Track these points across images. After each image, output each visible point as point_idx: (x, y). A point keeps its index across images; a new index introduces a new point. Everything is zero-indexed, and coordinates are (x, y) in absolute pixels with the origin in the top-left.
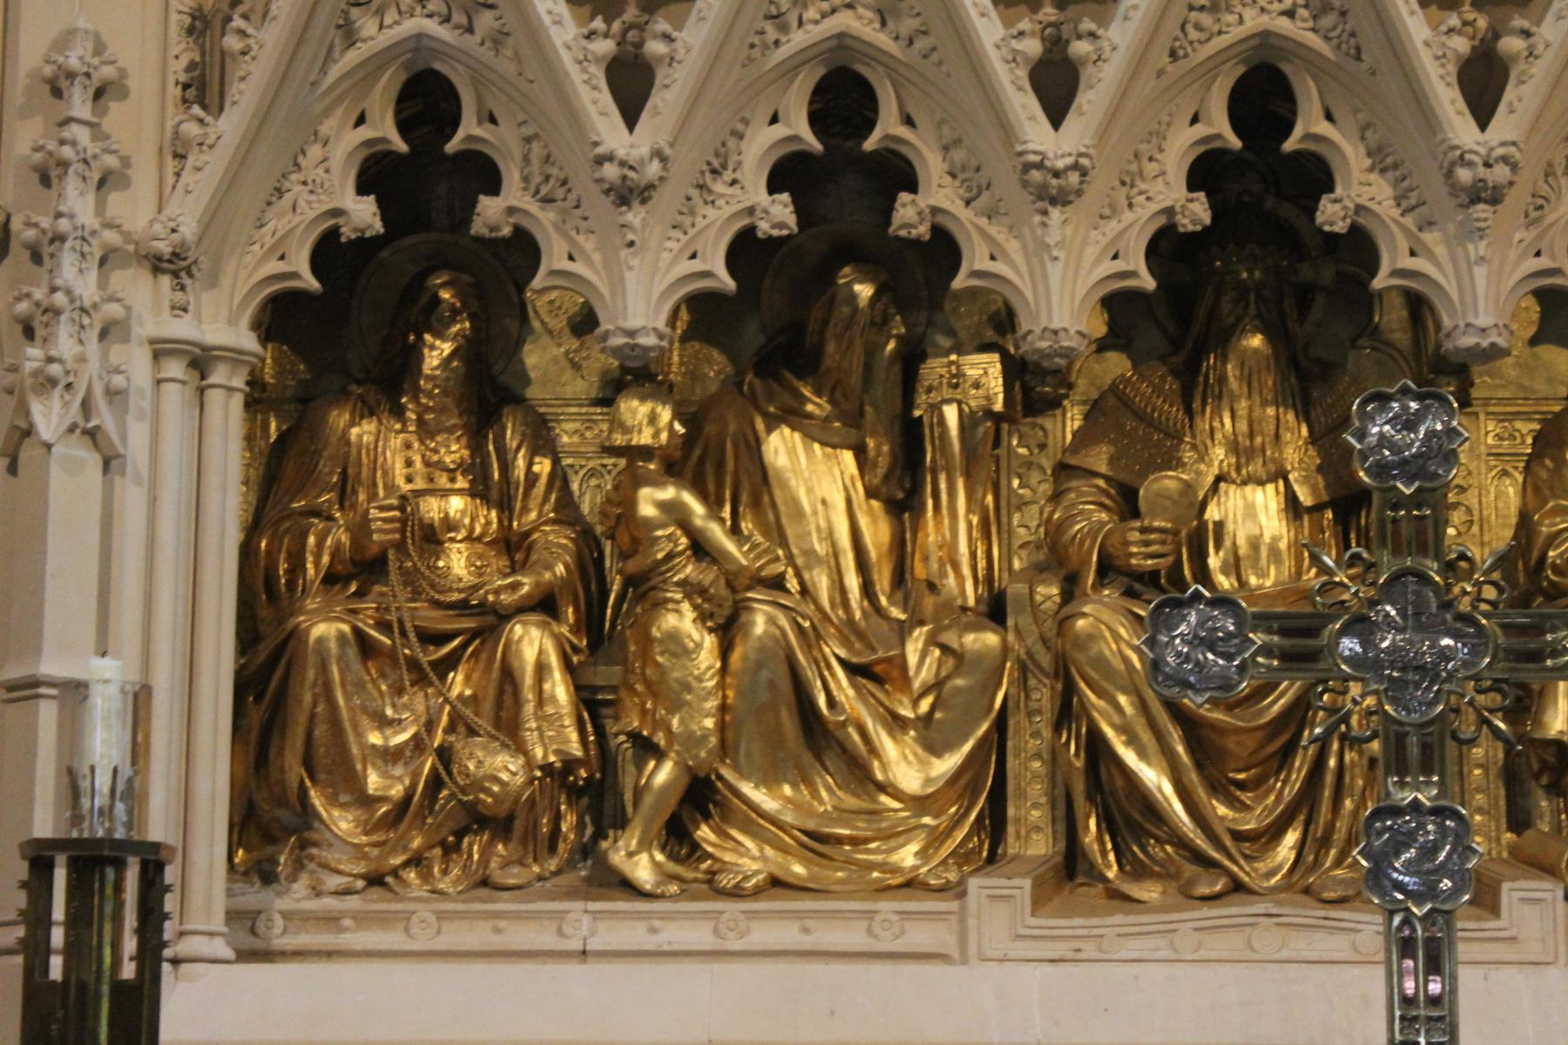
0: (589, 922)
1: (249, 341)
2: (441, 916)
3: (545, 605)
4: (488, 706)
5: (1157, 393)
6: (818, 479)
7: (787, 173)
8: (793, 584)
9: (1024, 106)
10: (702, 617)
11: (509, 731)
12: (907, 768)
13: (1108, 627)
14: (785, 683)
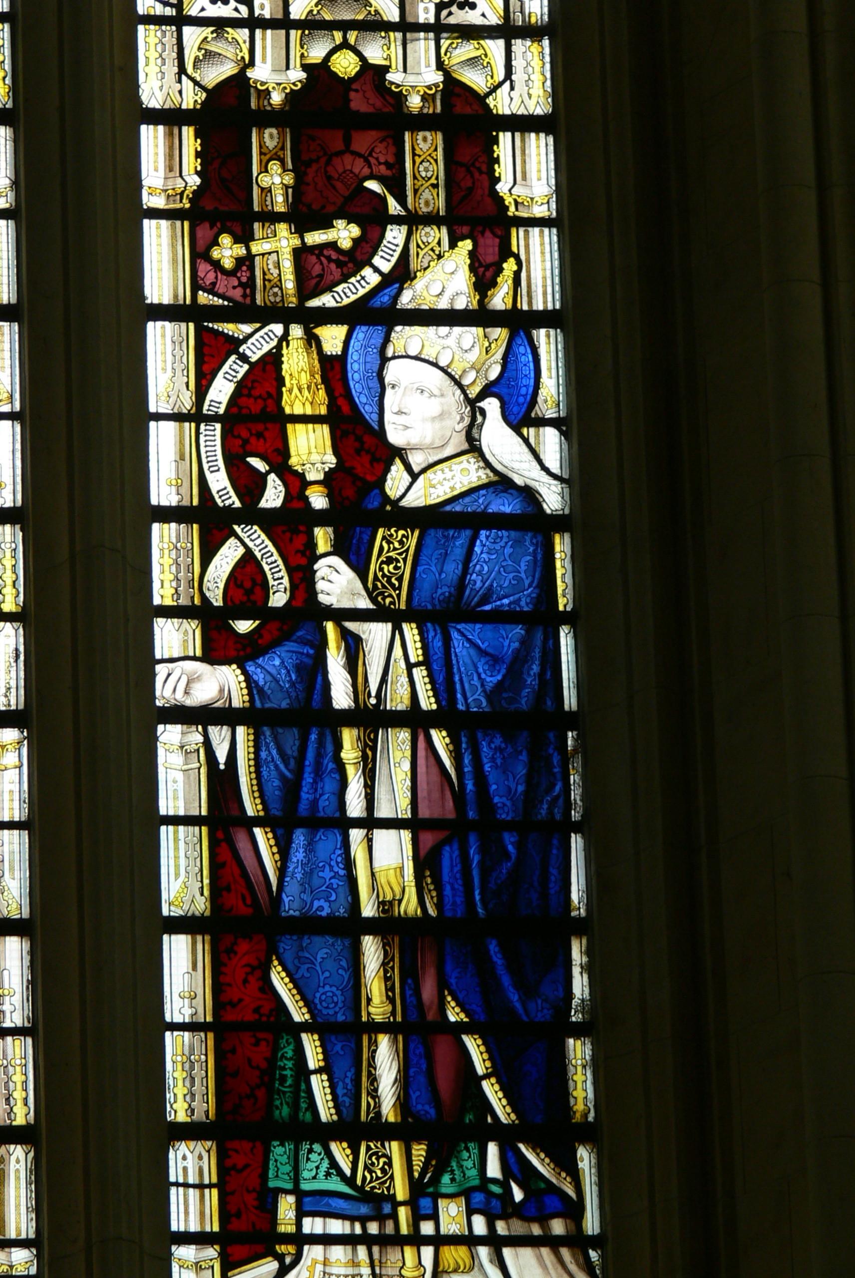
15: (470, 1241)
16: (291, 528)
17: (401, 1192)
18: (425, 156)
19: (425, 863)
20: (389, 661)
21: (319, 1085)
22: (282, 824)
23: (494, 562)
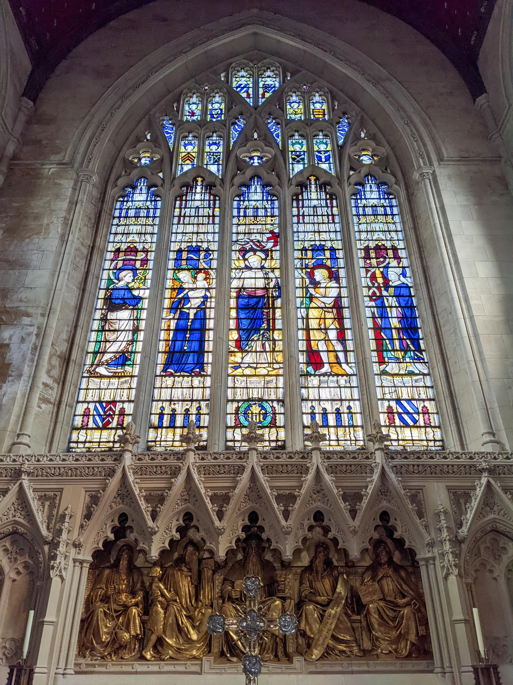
0: (139, 667)
1: (91, 559)
2: (112, 665)
3: (136, 605)
4: (125, 624)
8: (178, 600)
10: (162, 607)
11: (128, 630)
14: (174, 620)
15: (410, 362)
16: (379, 288)
17: (401, 357)
19: (400, 322)
20: (393, 301)
21: (389, 346)
22: (381, 318)
23: (404, 292)
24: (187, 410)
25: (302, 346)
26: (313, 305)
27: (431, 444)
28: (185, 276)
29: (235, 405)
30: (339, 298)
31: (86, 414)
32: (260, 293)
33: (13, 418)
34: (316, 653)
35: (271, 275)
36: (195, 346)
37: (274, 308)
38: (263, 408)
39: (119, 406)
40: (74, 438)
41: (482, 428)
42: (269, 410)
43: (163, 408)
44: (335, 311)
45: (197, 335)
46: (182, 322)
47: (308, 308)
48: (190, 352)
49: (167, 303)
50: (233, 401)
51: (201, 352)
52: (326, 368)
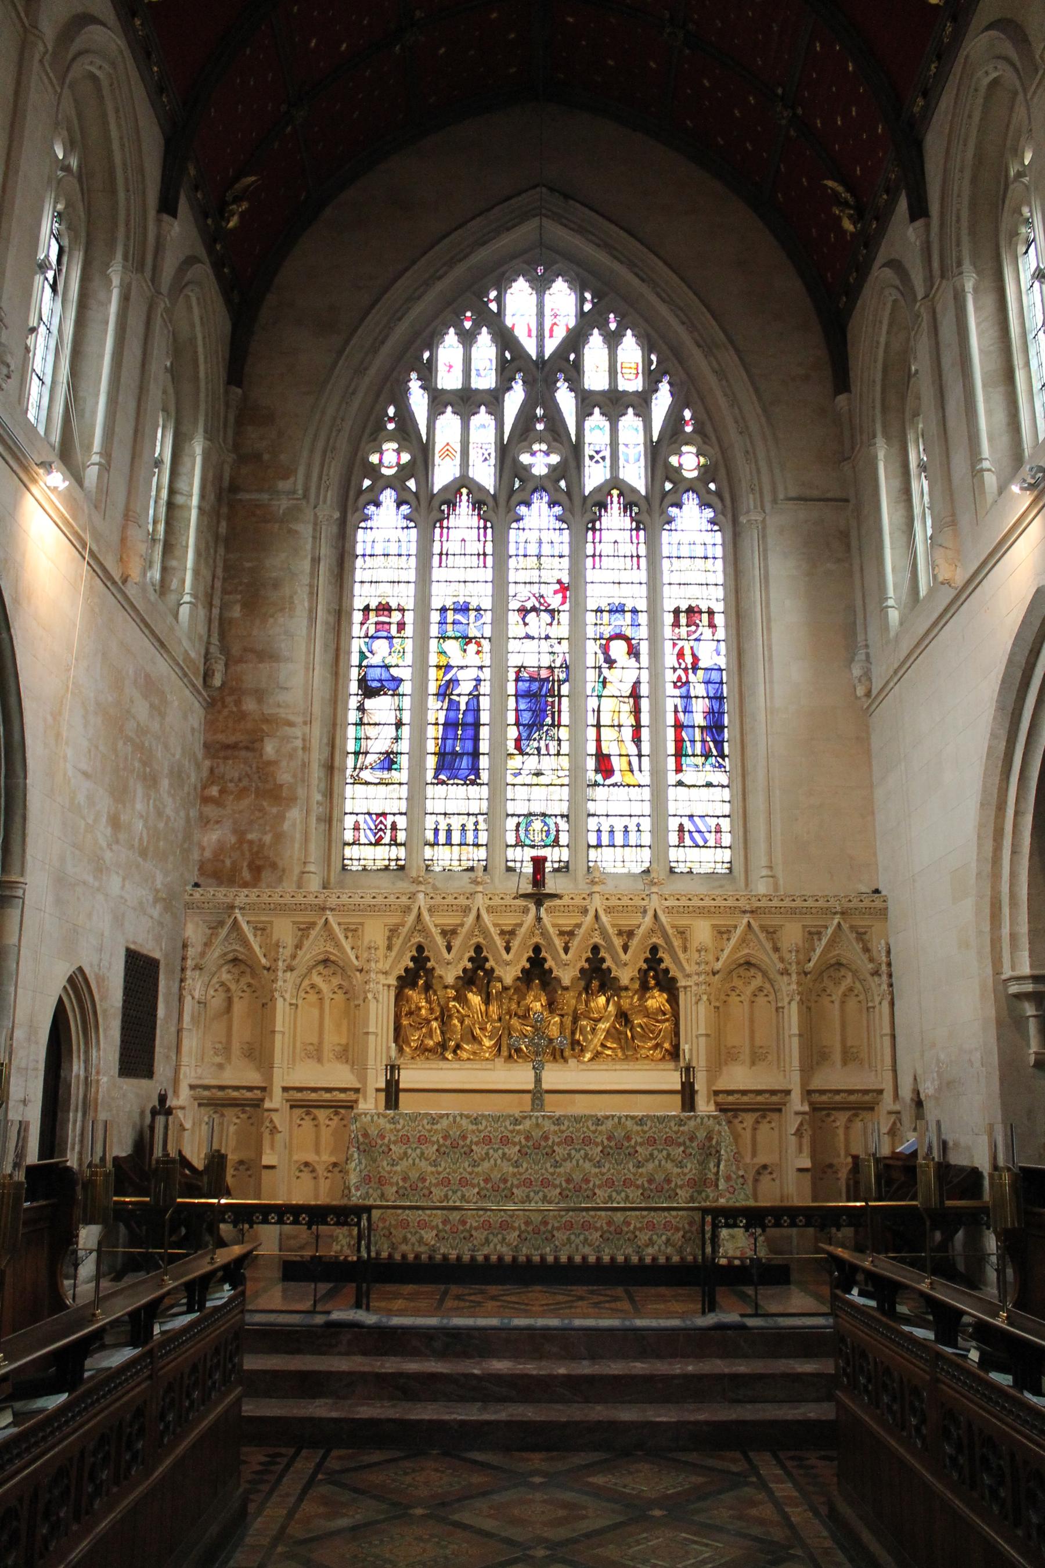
0: (443, 1064)
3: (436, 1019)
5: (523, 987)
6: (475, 999)
7: (471, 959)
9: (504, 952)
11: (431, 1037)
12: (487, 1043)
13: (514, 1021)
16: (686, 670)
18: (705, 617)
20: (699, 690)
22: (684, 712)
24: (463, 825)
25: (592, 748)
26: (606, 693)
27: (719, 866)
28: (452, 647)
29: (516, 820)
30: (637, 684)
31: (356, 828)
32: (544, 674)
33: (297, 846)
34: (588, 1055)
35: (557, 648)
36: (469, 746)
37: (560, 696)
38: (546, 824)
39: (390, 819)
40: (347, 855)
41: (764, 861)
42: (553, 827)
43: (437, 823)
44: (631, 700)
45: (470, 732)
46: (452, 714)
47: (600, 697)
48: (462, 754)
49: (433, 688)
50: (513, 815)
51: (476, 754)
52: (616, 778)
